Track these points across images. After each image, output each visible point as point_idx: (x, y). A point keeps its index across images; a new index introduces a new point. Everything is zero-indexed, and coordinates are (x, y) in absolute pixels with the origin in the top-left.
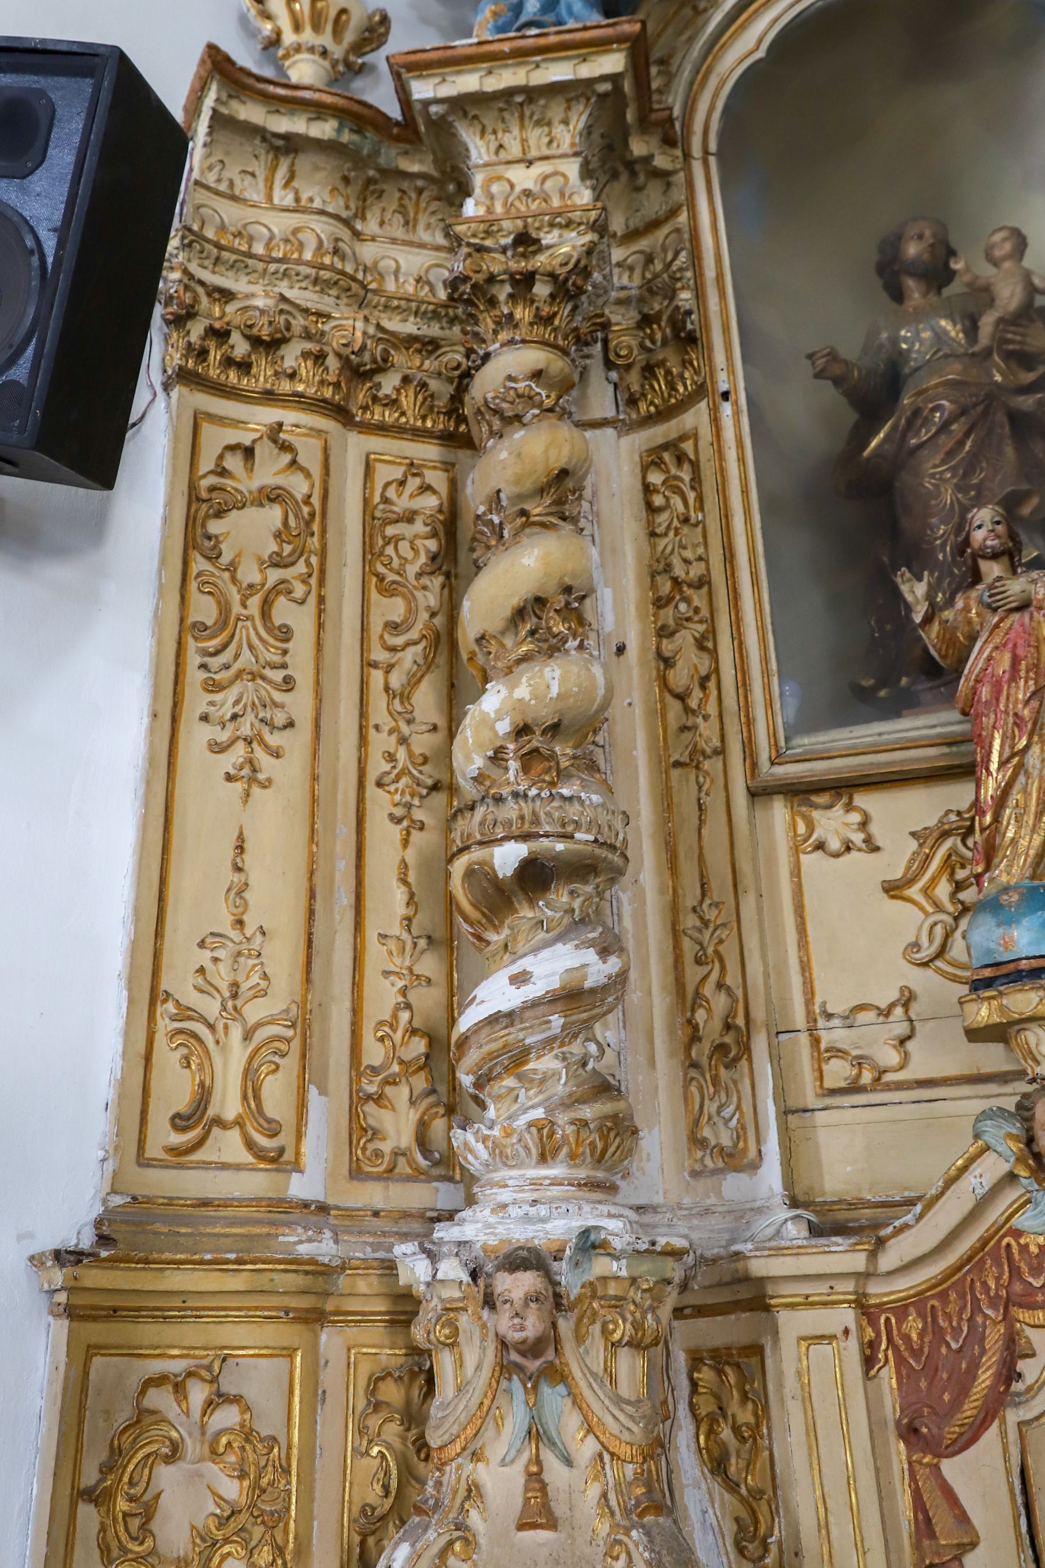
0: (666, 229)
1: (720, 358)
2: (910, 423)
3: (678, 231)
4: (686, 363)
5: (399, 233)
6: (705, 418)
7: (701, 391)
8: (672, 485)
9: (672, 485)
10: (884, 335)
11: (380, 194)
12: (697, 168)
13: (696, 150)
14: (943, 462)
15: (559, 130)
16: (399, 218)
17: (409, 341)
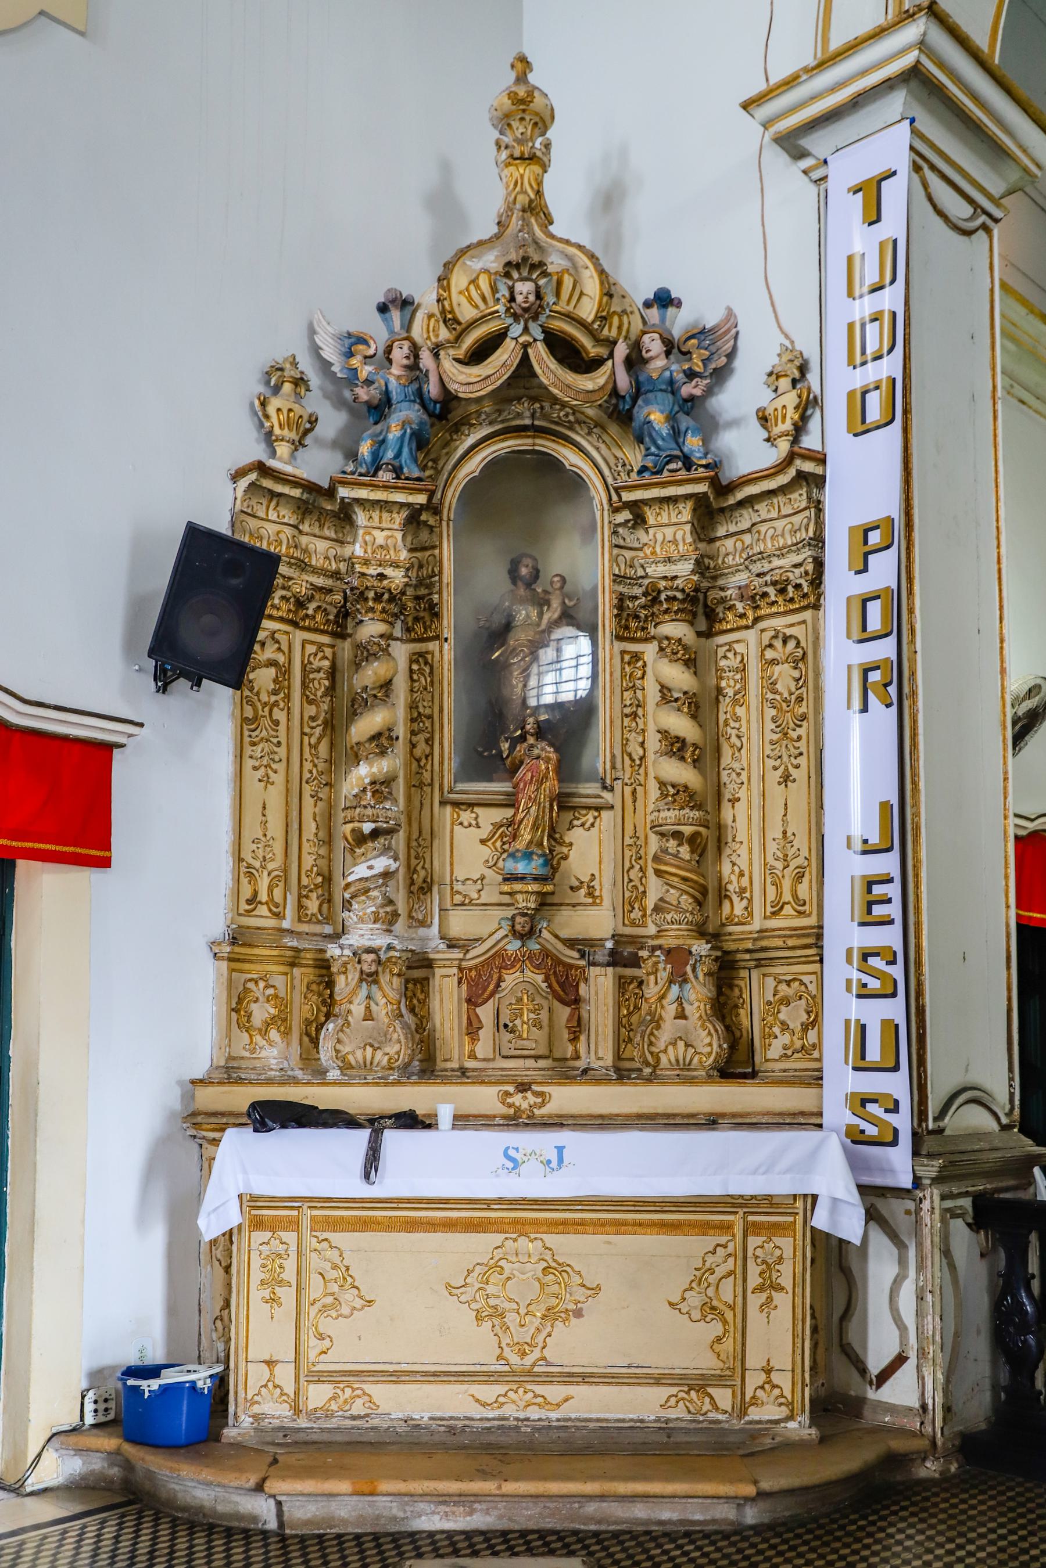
0: (429, 553)
1: (445, 623)
2: (511, 652)
3: (434, 556)
4: (432, 621)
5: (317, 531)
6: (437, 649)
7: (437, 638)
8: (421, 671)
9: (421, 671)
10: (507, 604)
11: (311, 513)
12: (444, 524)
13: (445, 518)
14: (521, 673)
15: (395, 515)
16: (317, 524)
17: (321, 589)
